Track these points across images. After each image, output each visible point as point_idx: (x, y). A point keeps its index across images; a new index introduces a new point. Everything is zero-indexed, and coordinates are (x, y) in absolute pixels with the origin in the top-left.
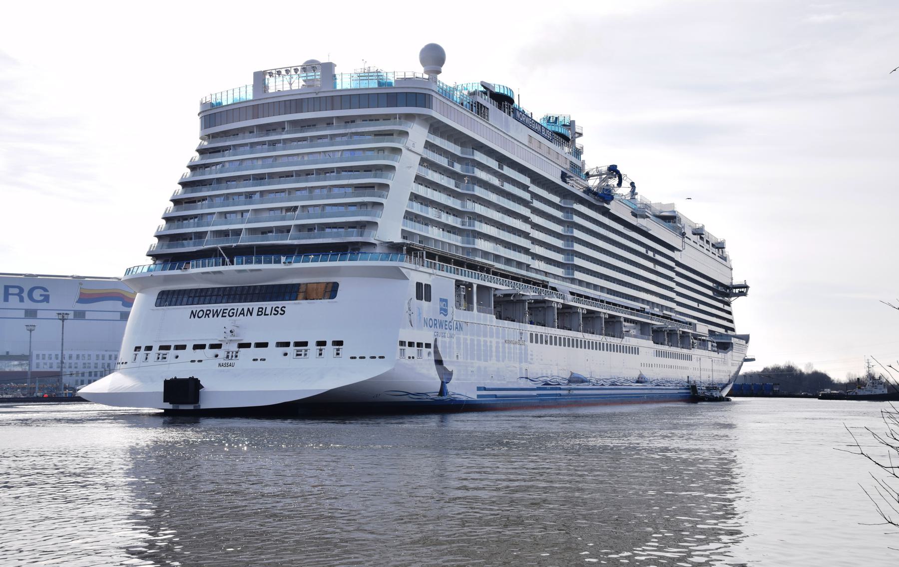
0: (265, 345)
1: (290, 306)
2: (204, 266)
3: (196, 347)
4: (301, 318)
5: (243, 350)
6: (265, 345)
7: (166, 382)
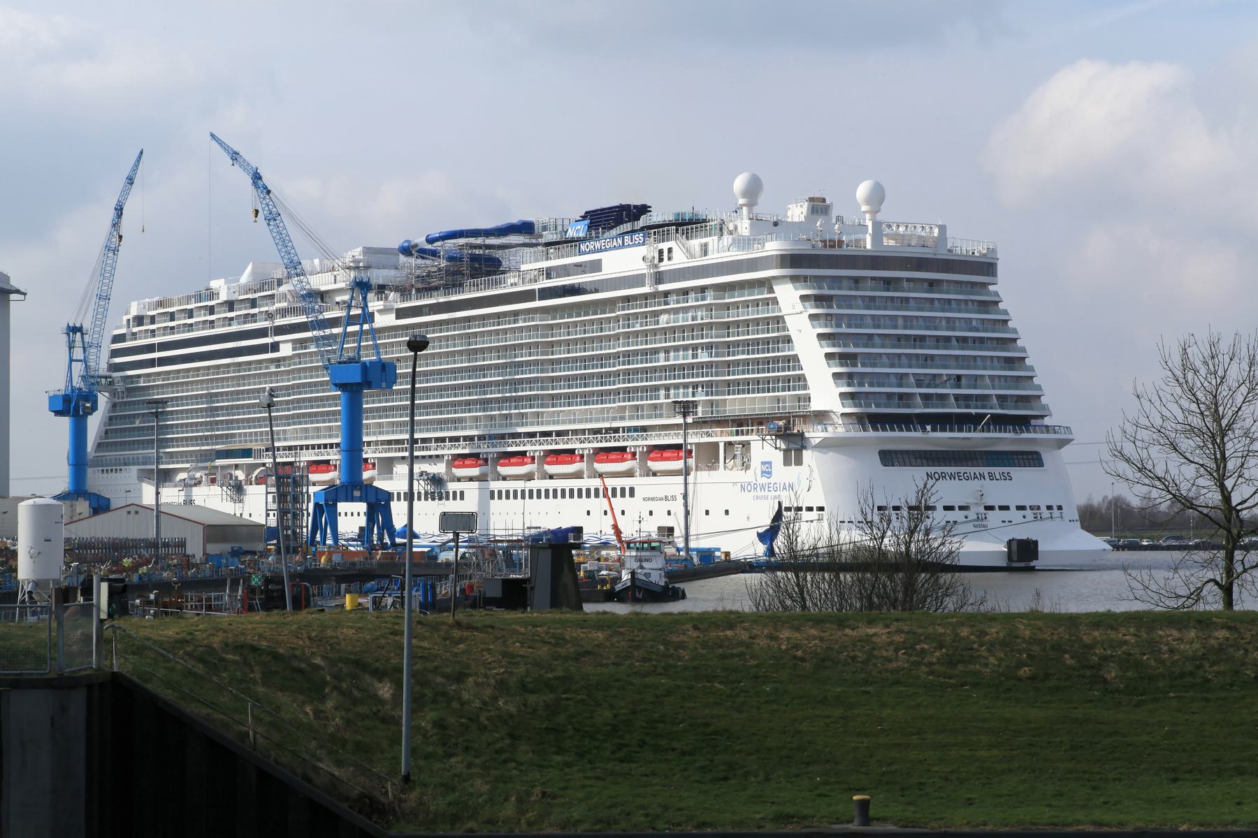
0: (1006, 508)
1: (1019, 473)
2: (951, 430)
3: (946, 508)
4: (1020, 485)
5: (990, 512)
6: (1006, 508)
7: (1036, 542)
